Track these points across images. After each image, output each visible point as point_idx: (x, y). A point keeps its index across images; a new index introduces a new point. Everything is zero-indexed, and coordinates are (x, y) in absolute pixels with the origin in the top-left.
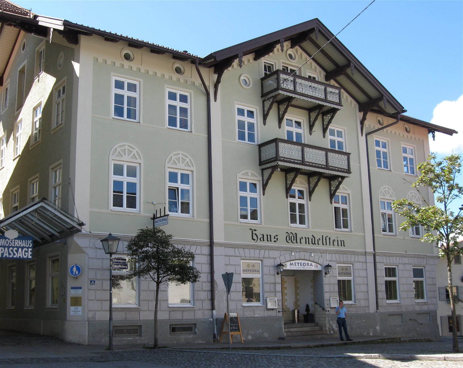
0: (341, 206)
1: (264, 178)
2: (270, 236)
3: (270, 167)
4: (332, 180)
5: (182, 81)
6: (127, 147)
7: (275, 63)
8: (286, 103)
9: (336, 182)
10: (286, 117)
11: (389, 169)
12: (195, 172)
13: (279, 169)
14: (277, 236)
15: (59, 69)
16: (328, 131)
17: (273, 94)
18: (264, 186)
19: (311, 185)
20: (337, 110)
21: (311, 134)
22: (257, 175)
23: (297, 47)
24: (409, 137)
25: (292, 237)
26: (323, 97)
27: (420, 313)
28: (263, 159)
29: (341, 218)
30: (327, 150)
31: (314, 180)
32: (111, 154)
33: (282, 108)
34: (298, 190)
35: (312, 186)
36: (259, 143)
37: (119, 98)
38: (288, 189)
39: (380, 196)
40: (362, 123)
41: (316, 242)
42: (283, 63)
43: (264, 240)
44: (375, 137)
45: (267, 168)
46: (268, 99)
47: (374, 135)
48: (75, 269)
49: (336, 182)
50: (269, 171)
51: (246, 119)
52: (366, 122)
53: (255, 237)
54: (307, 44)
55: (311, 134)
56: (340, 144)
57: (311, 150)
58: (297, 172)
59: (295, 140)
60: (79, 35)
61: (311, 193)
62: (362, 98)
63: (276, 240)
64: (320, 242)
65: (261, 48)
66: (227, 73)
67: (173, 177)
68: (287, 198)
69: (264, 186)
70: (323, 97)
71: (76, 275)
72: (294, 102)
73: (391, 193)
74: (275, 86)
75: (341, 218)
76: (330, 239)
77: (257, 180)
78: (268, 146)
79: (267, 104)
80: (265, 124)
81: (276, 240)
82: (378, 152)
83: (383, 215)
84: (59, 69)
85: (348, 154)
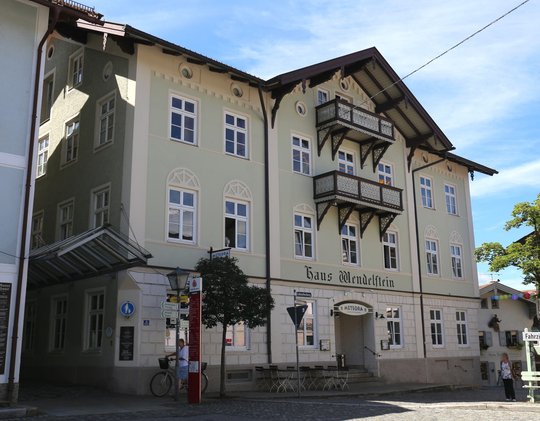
0: (391, 245)
1: (319, 212)
2: (324, 274)
3: (326, 201)
4: (382, 218)
5: (240, 104)
6: (184, 172)
7: (329, 92)
8: (342, 135)
9: (367, 216)
10: (340, 149)
11: (433, 207)
12: (200, 193)
13: (336, 203)
14: (331, 274)
15: (105, 80)
16: (378, 166)
17: (330, 124)
18: (319, 221)
19: (363, 222)
20: (391, 144)
21: (362, 168)
22: (313, 210)
23: (350, 77)
24: (451, 176)
25: (345, 276)
26: (377, 130)
27: (464, 359)
28: (319, 192)
29: (390, 258)
30: (382, 186)
31: (345, 211)
32: (224, 191)
33: (337, 139)
34: (305, 218)
35: (364, 222)
36: (314, 176)
37: (176, 118)
38: (341, 226)
39: (425, 236)
40: (409, 159)
41: (368, 283)
42: (337, 92)
43: (318, 279)
44: (420, 174)
45: (323, 202)
46: (324, 128)
47: (419, 172)
48: (127, 307)
49: (367, 216)
50: (325, 205)
51: (301, 149)
52: (413, 159)
53: (310, 275)
55: (362, 168)
56: (388, 179)
57: (367, 184)
58: (352, 207)
59: (346, 172)
60: (135, 45)
61: (362, 230)
62: (410, 133)
63: (329, 278)
64: (371, 282)
65: (318, 74)
66: (287, 99)
67: (230, 207)
68: (340, 234)
69: (319, 221)
70: (377, 130)
71: (128, 313)
72: (349, 134)
73: (435, 232)
74: (332, 115)
75: (390, 258)
76: (380, 279)
77: (312, 214)
78: (324, 179)
79: (323, 135)
80: (319, 155)
81: (329, 278)
82: (423, 190)
83: (429, 254)
84: (105, 80)
85: (400, 191)
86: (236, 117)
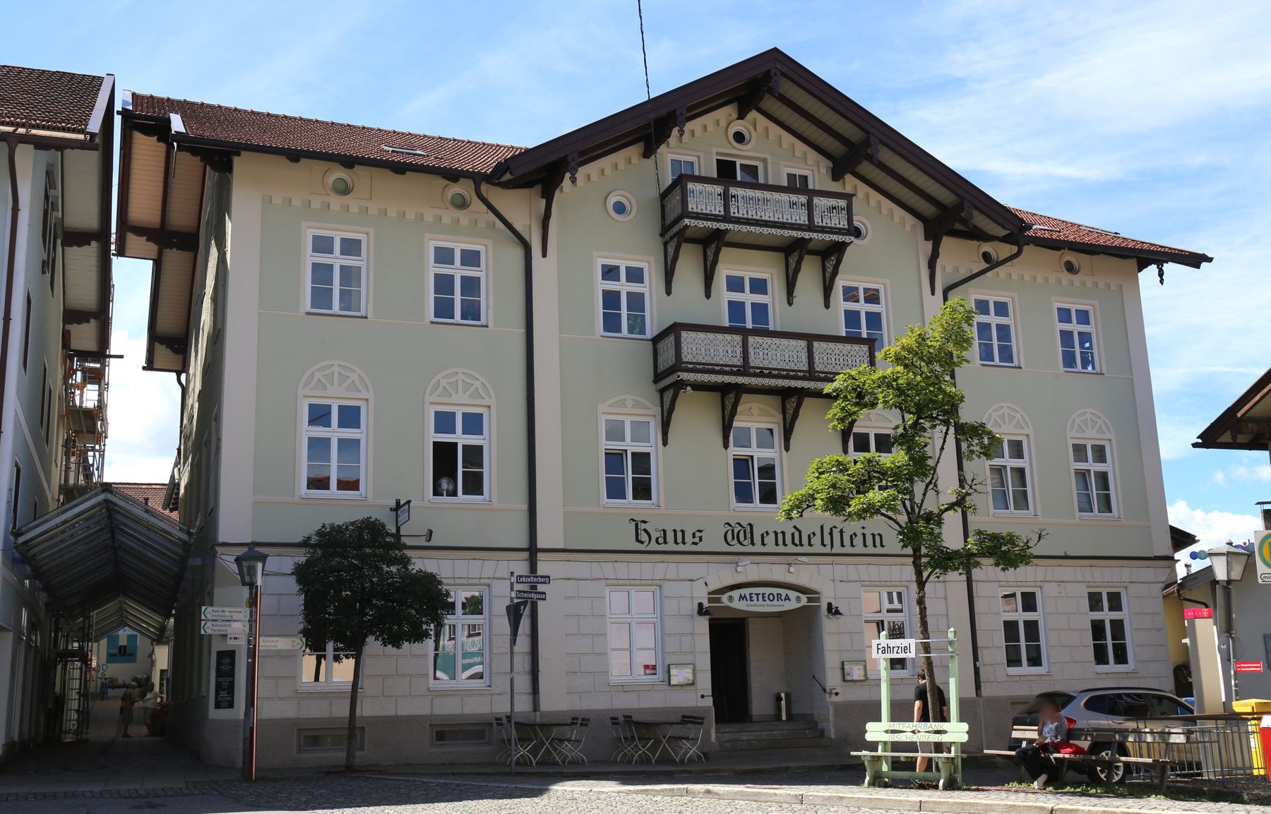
2: (683, 531)
23: (754, 114)
42: (718, 154)
43: (665, 542)
53: (644, 537)
54: (769, 103)
55: (790, 304)
62: (928, 209)
63: (697, 540)
65: (648, 125)
76: (841, 532)
80: (669, 292)
86: (992, 300)
